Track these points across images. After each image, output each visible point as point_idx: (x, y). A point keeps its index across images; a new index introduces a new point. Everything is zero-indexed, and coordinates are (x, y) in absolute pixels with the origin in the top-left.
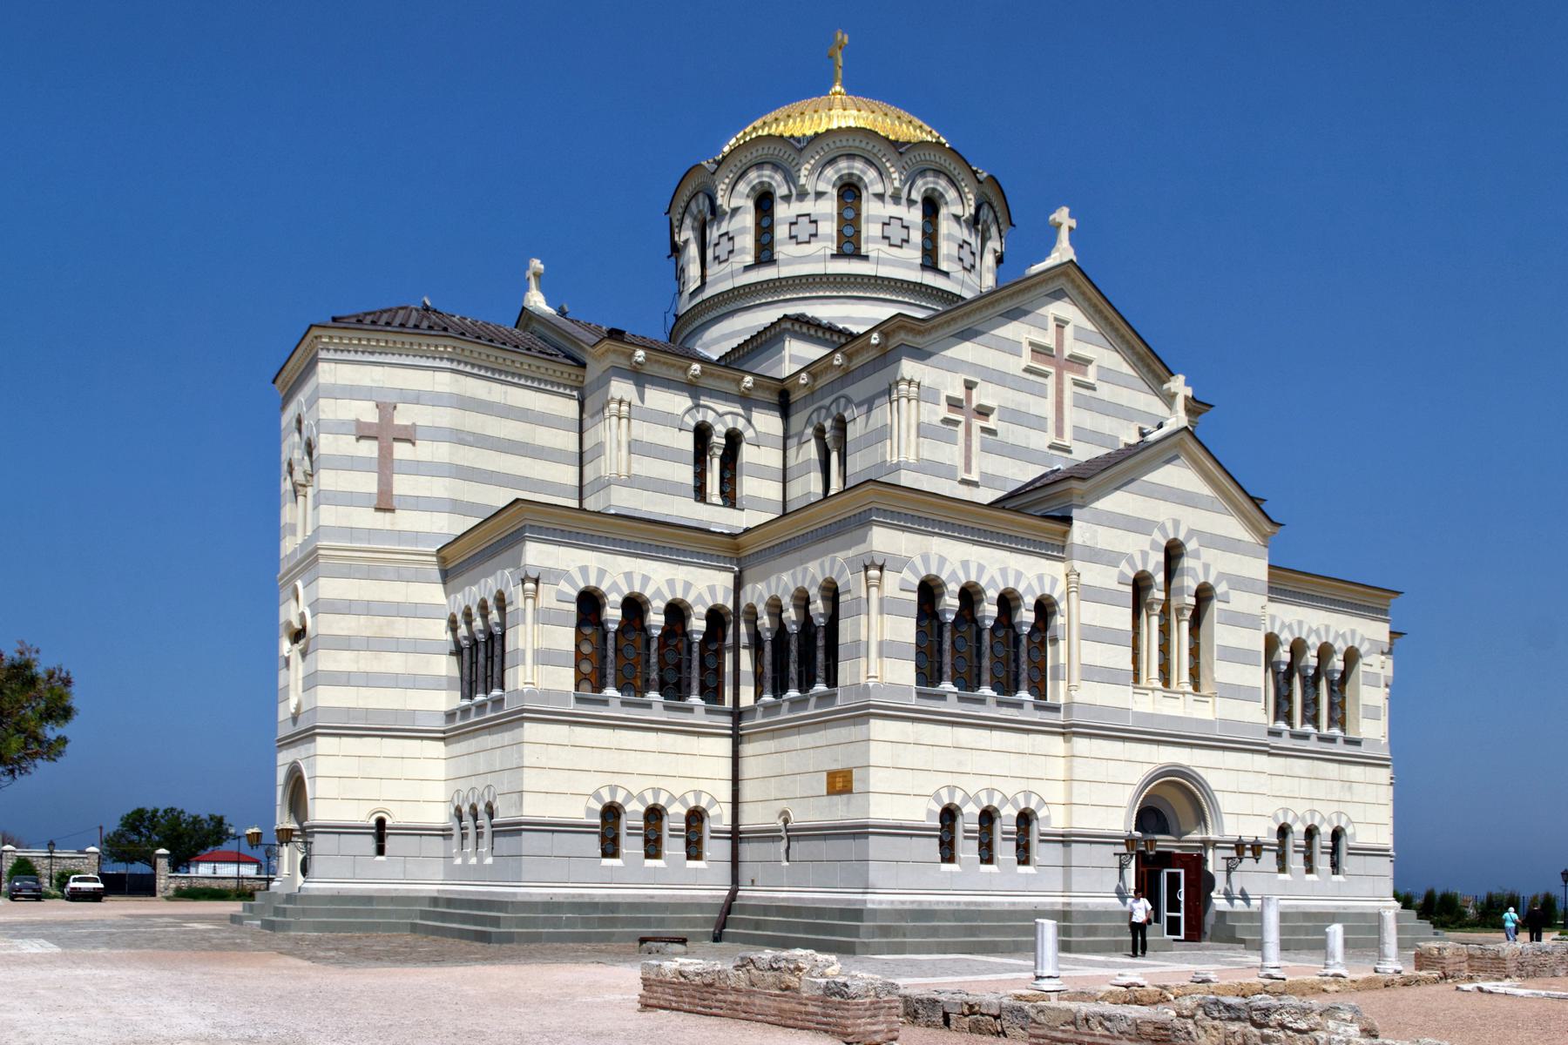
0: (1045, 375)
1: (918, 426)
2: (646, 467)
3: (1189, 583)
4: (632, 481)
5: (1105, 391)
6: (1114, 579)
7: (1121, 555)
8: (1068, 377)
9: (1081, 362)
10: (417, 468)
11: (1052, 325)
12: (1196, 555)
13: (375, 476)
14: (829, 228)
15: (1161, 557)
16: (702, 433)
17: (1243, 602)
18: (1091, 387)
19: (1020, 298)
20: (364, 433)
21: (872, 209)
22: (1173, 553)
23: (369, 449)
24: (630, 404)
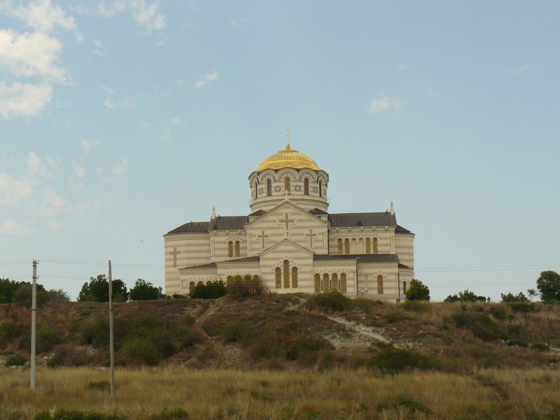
0: (283, 224)
1: (251, 242)
2: (217, 252)
3: (291, 268)
4: (215, 256)
5: (299, 224)
6: (273, 270)
7: (273, 265)
8: (289, 223)
9: (292, 221)
10: (181, 259)
11: (285, 214)
12: (292, 262)
13: (173, 261)
14: (265, 190)
15: (283, 264)
16: (230, 243)
17: (304, 269)
18: (296, 224)
19: (275, 211)
20: (171, 253)
21: (273, 185)
22: (286, 262)
23: (172, 257)
24: (214, 241)
